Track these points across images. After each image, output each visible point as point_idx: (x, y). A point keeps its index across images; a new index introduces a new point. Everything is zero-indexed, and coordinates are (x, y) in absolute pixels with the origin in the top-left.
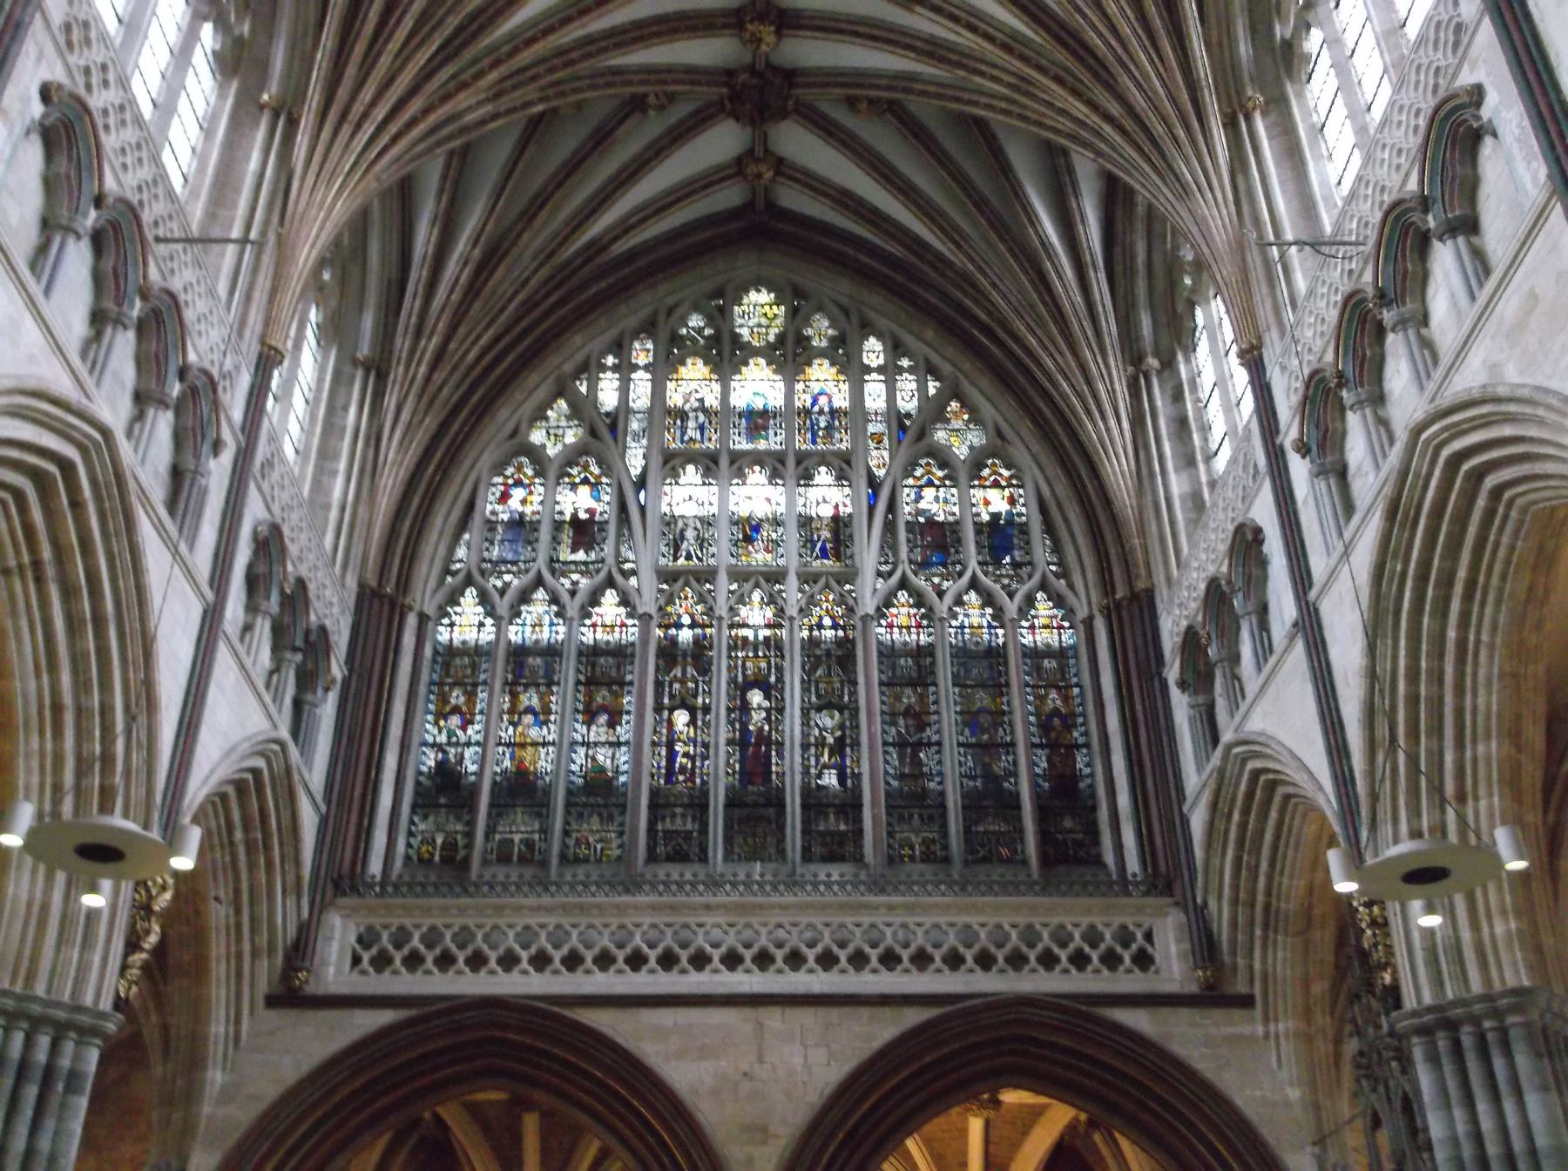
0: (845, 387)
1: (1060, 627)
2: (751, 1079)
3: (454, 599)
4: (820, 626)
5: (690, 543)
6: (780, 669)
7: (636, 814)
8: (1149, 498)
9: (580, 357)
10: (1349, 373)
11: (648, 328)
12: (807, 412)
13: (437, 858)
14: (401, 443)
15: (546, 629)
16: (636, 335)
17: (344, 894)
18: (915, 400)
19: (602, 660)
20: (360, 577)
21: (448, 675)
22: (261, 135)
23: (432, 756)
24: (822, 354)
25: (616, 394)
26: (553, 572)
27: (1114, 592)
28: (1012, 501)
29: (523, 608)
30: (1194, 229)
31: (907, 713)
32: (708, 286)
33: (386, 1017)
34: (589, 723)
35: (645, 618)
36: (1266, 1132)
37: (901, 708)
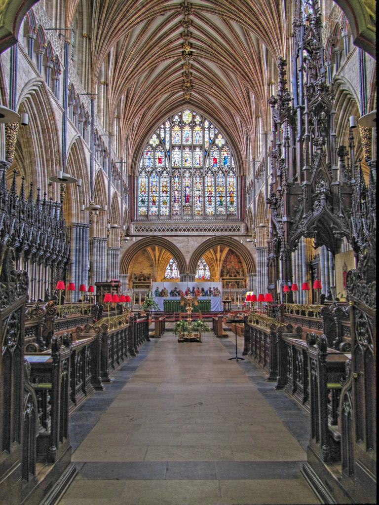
0: (202, 132)
3: (141, 172)
11: (169, 119)
28: (228, 154)
33: (140, 238)
34: (163, 193)
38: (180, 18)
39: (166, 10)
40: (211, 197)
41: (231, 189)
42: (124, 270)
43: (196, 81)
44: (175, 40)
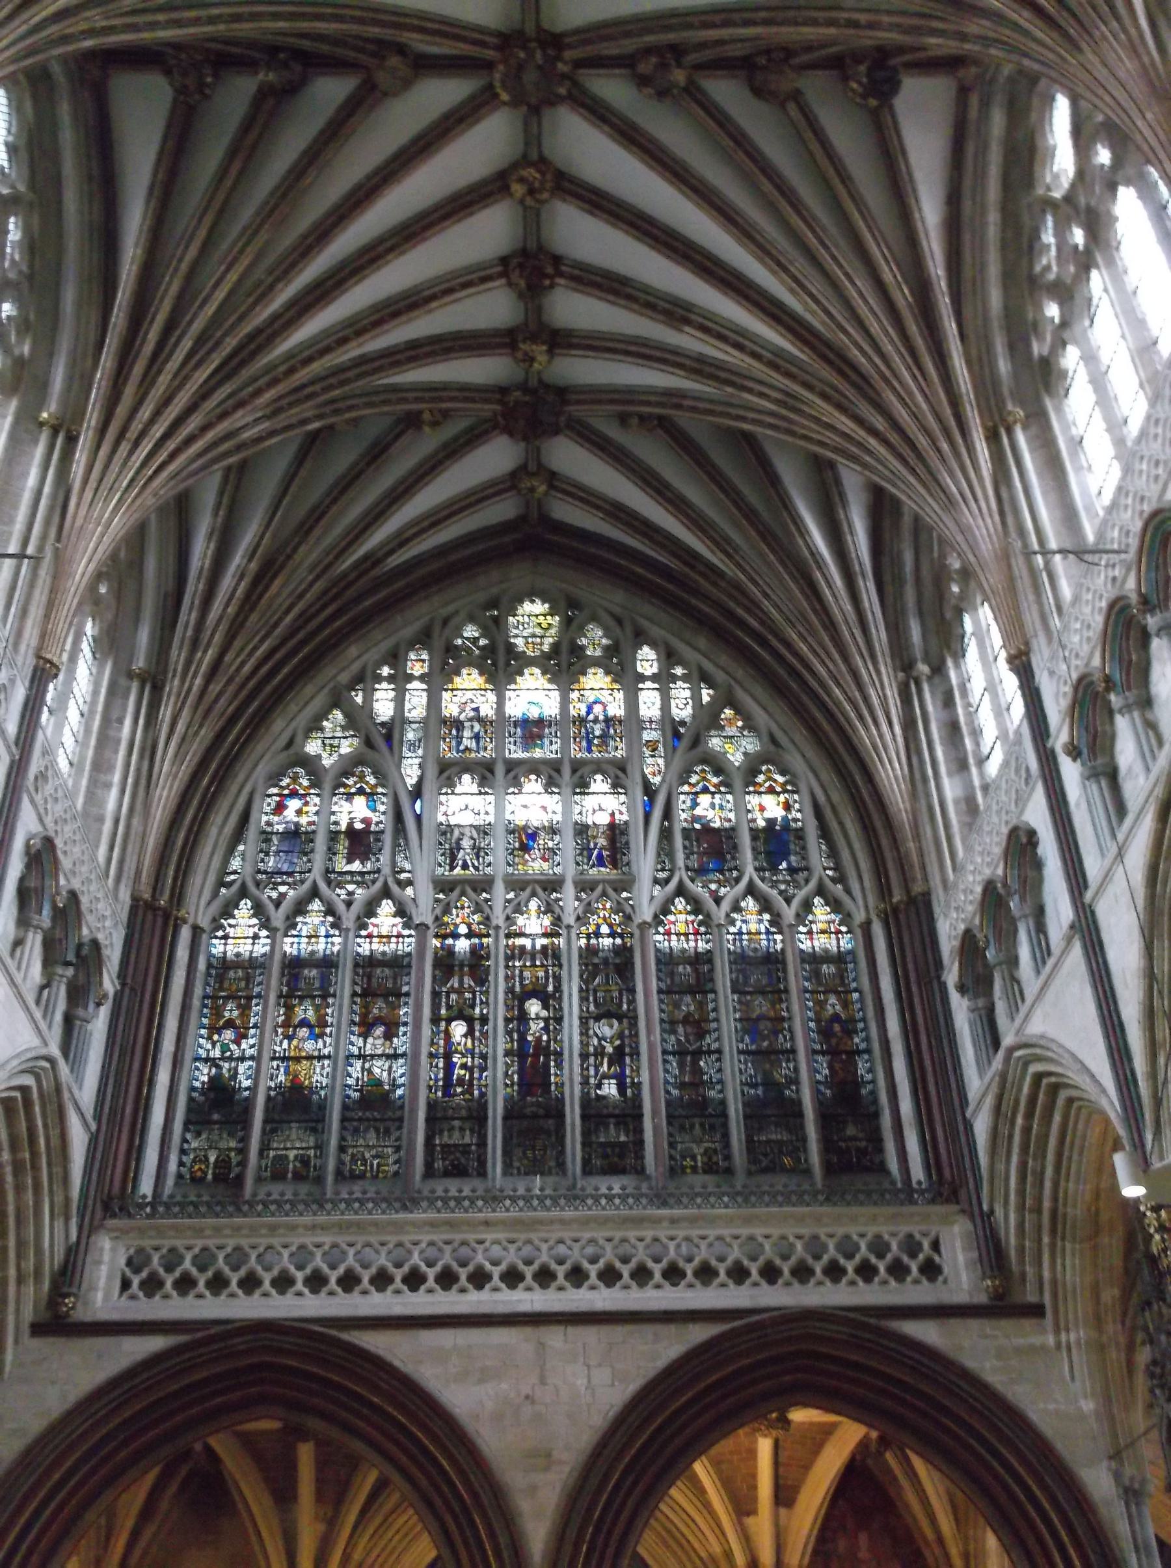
0: (620, 695)
1: (838, 932)
2: (533, 1402)
3: (227, 911)
4: (597, 934)
5: (465, 853)
6: (557, 979)
7: (413, 1131)
8: (923, 802)
9: (355, 667)
10: (1117, 677)
11: (423, 639)
12: (581, 721)
13: (210, 1177)
14: (176, 755)
15: (322, 940)
16: (411, 646)
17: (114, 1216)
18: (689, 707)
19: (379, 971)
20: (134, 890)
21: (221, 989)
22: (39, 451)
23: (206, 1071)
24: (596, 663)
25: (391, 705)
26: (329, 883)
27: (891, 895)
28: (787, 807)
29: (299, 919)
30: (960, 538)
31: (687, 1020)
32: (481, 597)
33: (156, 1344)
34: (365, 1035)
35: (422, 928)
36: (1059, 1446)
37: (679, 1015)
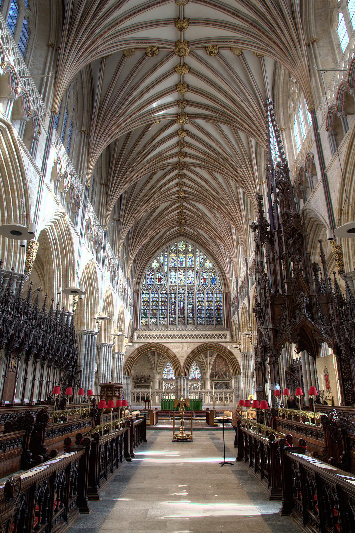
3: (144, 290)
28: (215, 275)
32: (175, 242)
33: (142, 344)
38: (176, 172)
39: (166, 166)
40: (201, 309)
41: (218, 303)
42: (127, 372)
43: (189, 218)
44: (172, 188)
